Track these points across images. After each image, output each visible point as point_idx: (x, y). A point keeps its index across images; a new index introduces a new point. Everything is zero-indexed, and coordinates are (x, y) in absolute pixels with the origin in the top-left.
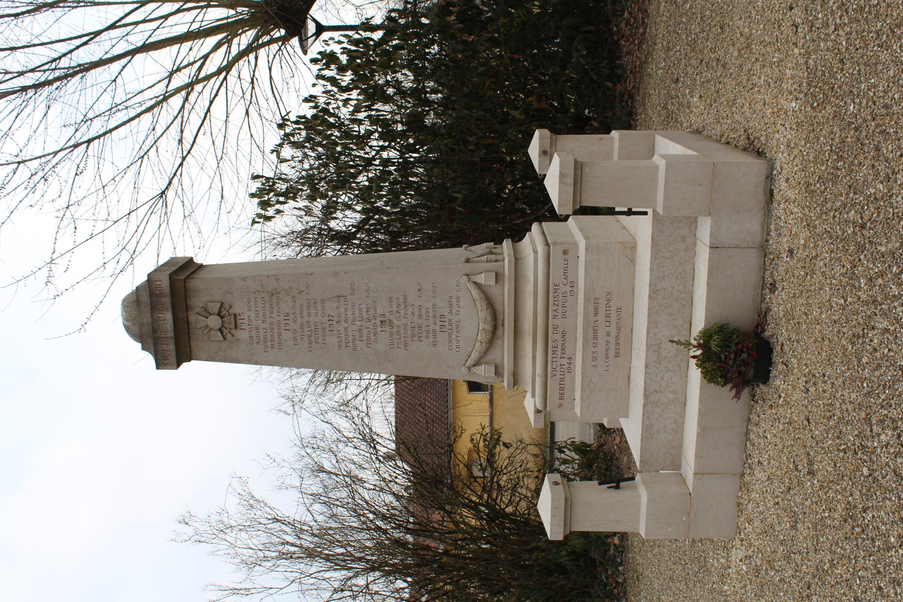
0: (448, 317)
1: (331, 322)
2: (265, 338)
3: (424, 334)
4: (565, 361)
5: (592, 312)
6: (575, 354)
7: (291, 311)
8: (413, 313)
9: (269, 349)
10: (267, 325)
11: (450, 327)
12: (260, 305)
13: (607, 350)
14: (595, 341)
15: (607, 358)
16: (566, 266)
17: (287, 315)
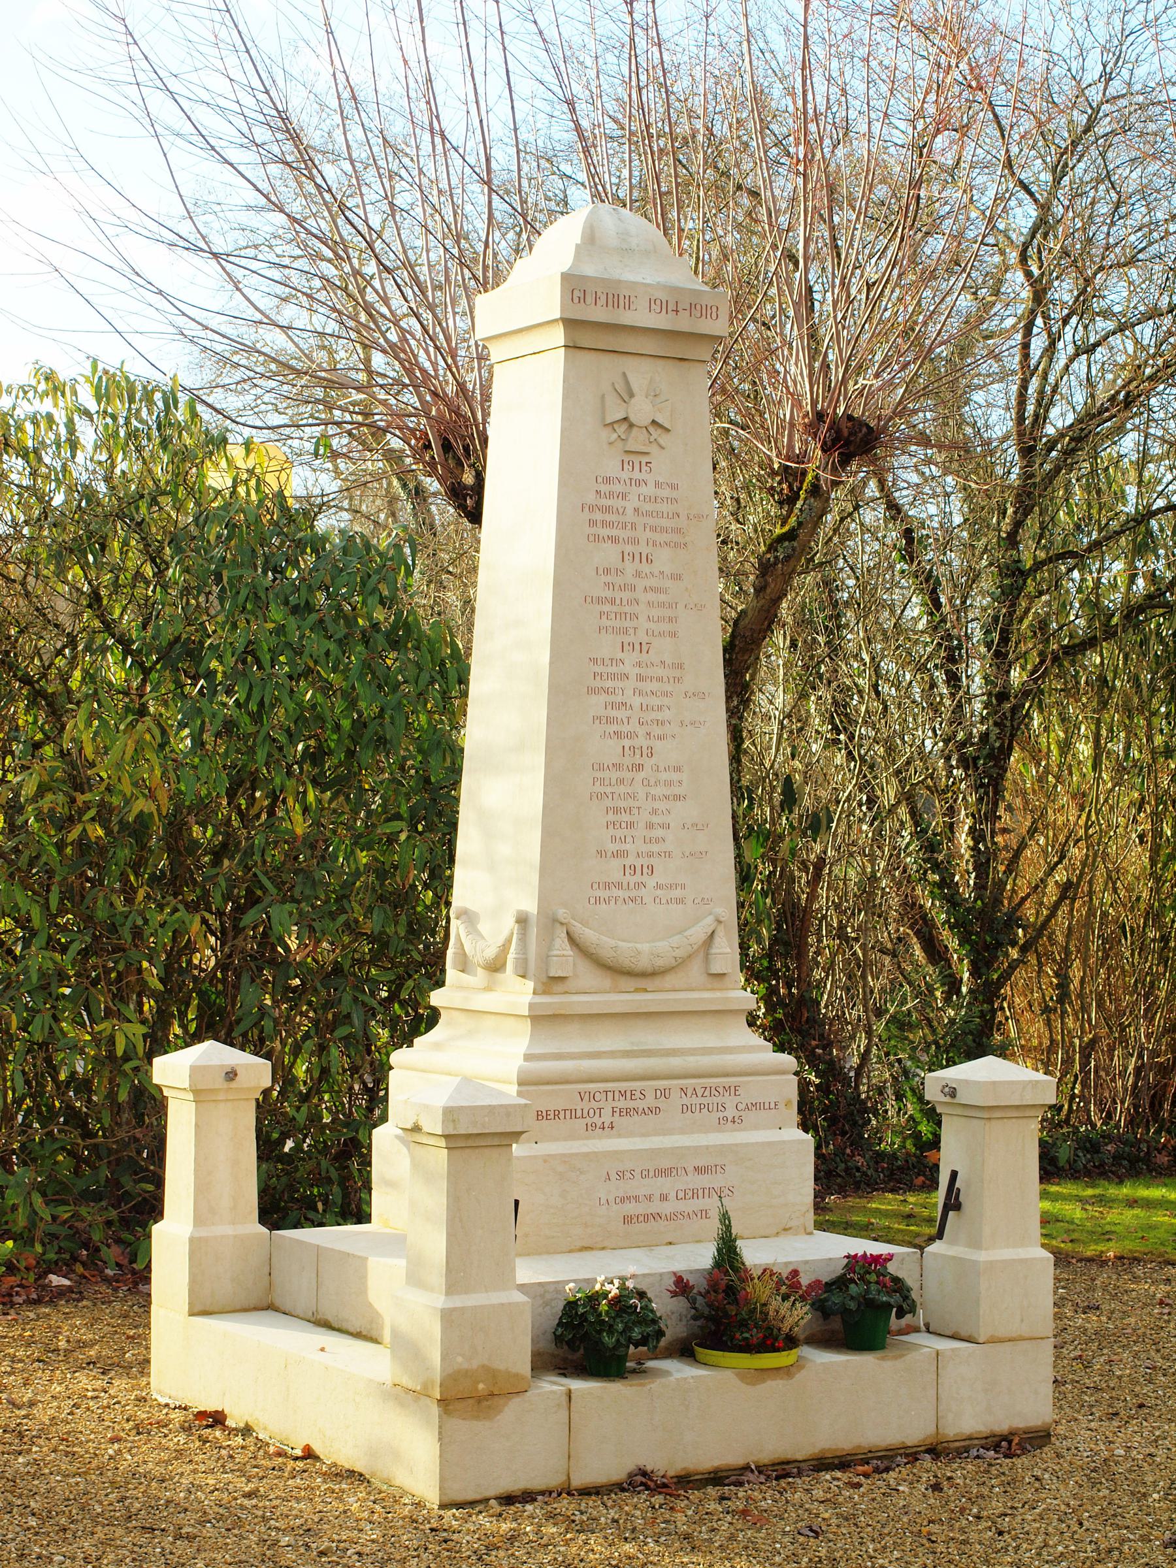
0: (651, 882)
1: (637, 647)
2: (607, 510)
3: (619, 833)
4: (607, 1118)
5: (700, 1163)
6: (619, 1136)
7: (656, 567)
8: (654, 812)
9: (587, 515)
10: (630, 516)
11: (632, 886)
12: (664, 508)
13: (636, 1198)
14: (651, 1174)
15: (623, 1200)
16: (767, 1106)
17: (649, 560)
